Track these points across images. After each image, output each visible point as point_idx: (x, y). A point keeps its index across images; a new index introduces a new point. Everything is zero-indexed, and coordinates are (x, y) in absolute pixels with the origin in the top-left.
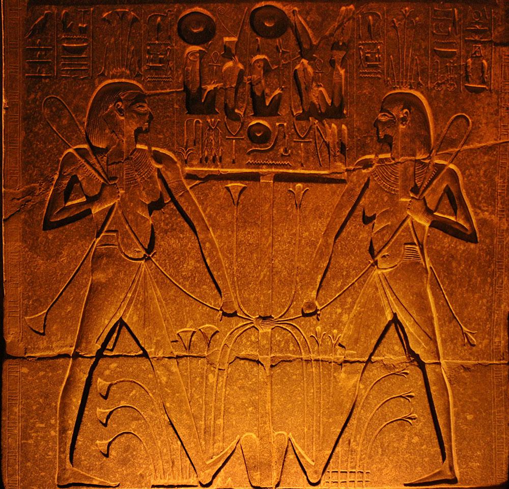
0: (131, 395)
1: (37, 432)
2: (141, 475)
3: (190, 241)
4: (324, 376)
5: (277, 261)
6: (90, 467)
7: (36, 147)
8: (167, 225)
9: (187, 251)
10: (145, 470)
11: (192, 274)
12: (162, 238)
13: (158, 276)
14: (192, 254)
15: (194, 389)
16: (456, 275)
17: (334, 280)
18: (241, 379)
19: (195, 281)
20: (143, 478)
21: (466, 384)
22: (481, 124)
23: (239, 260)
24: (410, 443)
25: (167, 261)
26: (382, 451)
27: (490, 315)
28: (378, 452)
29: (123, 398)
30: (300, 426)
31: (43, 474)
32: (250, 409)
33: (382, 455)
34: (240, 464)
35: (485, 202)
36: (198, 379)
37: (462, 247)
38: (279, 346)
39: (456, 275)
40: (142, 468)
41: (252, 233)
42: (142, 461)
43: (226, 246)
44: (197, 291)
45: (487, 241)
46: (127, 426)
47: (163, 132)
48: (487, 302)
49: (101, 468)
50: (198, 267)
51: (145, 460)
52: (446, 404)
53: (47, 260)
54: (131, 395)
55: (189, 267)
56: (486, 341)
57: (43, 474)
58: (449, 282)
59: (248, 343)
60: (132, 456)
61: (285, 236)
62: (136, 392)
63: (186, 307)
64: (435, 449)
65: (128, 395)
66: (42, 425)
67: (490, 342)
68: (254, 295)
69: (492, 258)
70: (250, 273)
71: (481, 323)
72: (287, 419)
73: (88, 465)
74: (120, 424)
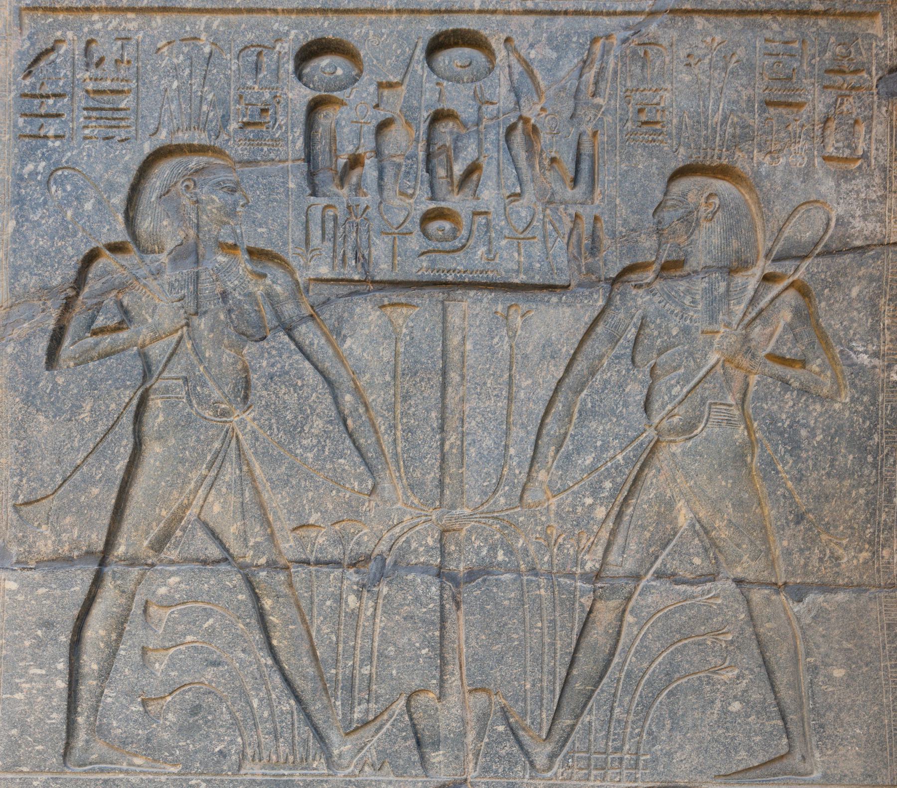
0: (206, 625)
1: (31, 682)
2: (221, 752)
3: (314, 390)
4: (562, 602)
5: (473, 423)
6: (126, 738)
7: (35, 244)
8: (273, 365)
9: (310, 406)
10: (228, 745)
11: (319, 442)
12: (264, 385)
13: (257, 444)
14: (318, 411)
15: (322, 618)
16: (807, 451)
17: (579, 454)
18: (408, 605)
19: (324, 451)
20: (225, 757)
21: (829, 620)
22: (853, 217)
23: (405, 420)
24: (725, 712)
25: (273, 421)
26: (673, 723)
27: (873, 514)
28: (664, 725)
29: (190, 632)
30: (518, 680)
31: (40, 747)
32: (424, 652)
33: (671, 730)
34: (405, 739)
35: (862, 339)
36: (328, 603)
37: (818, 407)
38: (477, 554)
39: (807, 451)
40: (223, 741)
41: (429, 379)
42: (222, 730)
43: (380, 400)
44: (328, 466)
45: (865, 399)
46: (197, 675)
47: (266, 223)
48: (867, 494)
49: (148, 740)
50: (331, 432)
51: (229, 728)
52: (792, 651)
53: (54, 417)
54: (206, 625)
55: (313, 430)
56: (865, 555)
57: (40, 747)
58: (794, 461)
59: (421, 549)
60: (206, 722)
61: (489, 385)
62: (216, 621)
63: (307, 491)
64: (774, 722)
65: (201, 627)
66: (39, 671)
67: (873, 557)
68: (432, 475)
69: (876, 425)
70: (425, 441)
71: (856, 526)
72: (492, 669)
73: (124, 736)
74: (183, 672)
